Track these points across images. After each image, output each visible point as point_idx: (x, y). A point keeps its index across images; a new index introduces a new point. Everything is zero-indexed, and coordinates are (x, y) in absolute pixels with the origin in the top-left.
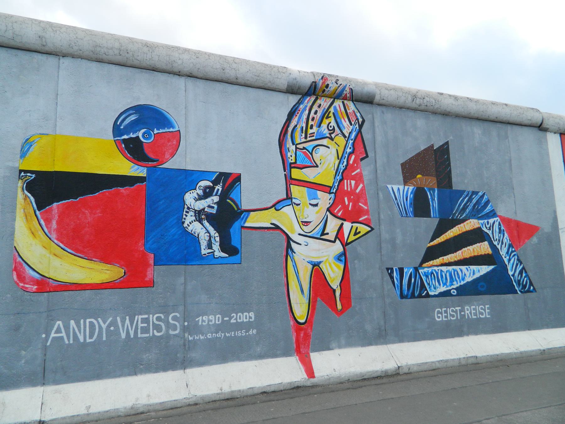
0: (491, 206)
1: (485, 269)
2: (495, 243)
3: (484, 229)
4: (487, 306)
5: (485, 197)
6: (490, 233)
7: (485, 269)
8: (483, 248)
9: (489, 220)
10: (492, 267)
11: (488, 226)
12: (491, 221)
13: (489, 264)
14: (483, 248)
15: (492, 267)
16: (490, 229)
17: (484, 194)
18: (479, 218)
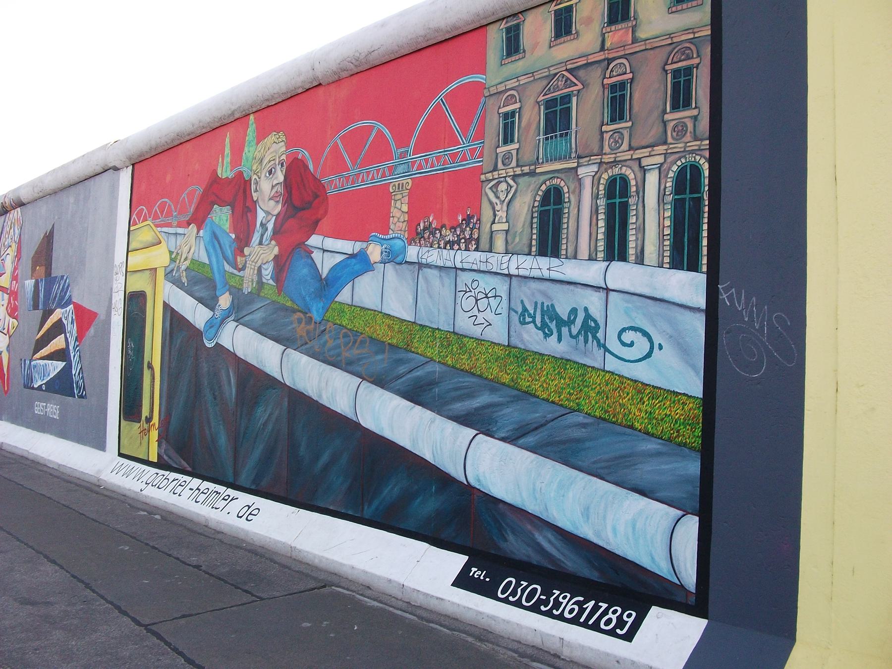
0: (70, 292)
1: (60, 365)
2: (68, 335)
3: (63, 320)
4: (58, 407)
5: (67, 281)
6: (66, 323)
7: (60, 365)
8: (58, 343)
9: (67, 309)
10: (65, 363)
11: (66, 316)
12: (68, 309)
13: (63, 361)
14: (58, 343)
15: (65, 363)
16: (66, 320)
17: (67, 278)
18: (63, 307)
